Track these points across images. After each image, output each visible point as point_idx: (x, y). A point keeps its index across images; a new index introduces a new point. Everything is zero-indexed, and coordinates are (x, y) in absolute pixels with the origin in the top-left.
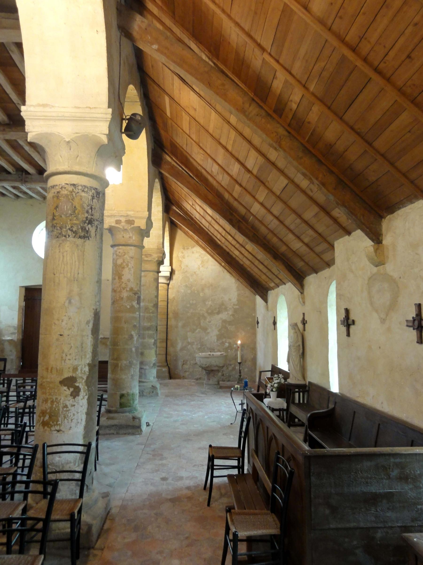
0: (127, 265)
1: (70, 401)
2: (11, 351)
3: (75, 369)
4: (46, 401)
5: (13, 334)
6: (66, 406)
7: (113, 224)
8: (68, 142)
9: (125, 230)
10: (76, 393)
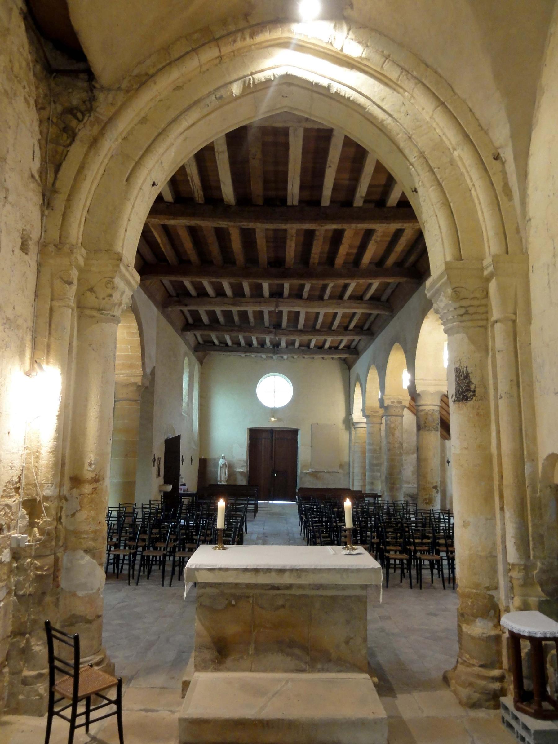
0: (397, 428)
1: (436, 495)
2: (242, 480)
3: (437, 483)
4: (427, 494)
5: (243, 466)
6: (435, 497)
7: (390, 404)
8: (432, 394)
9: (396, 407)
10: (437, 492)
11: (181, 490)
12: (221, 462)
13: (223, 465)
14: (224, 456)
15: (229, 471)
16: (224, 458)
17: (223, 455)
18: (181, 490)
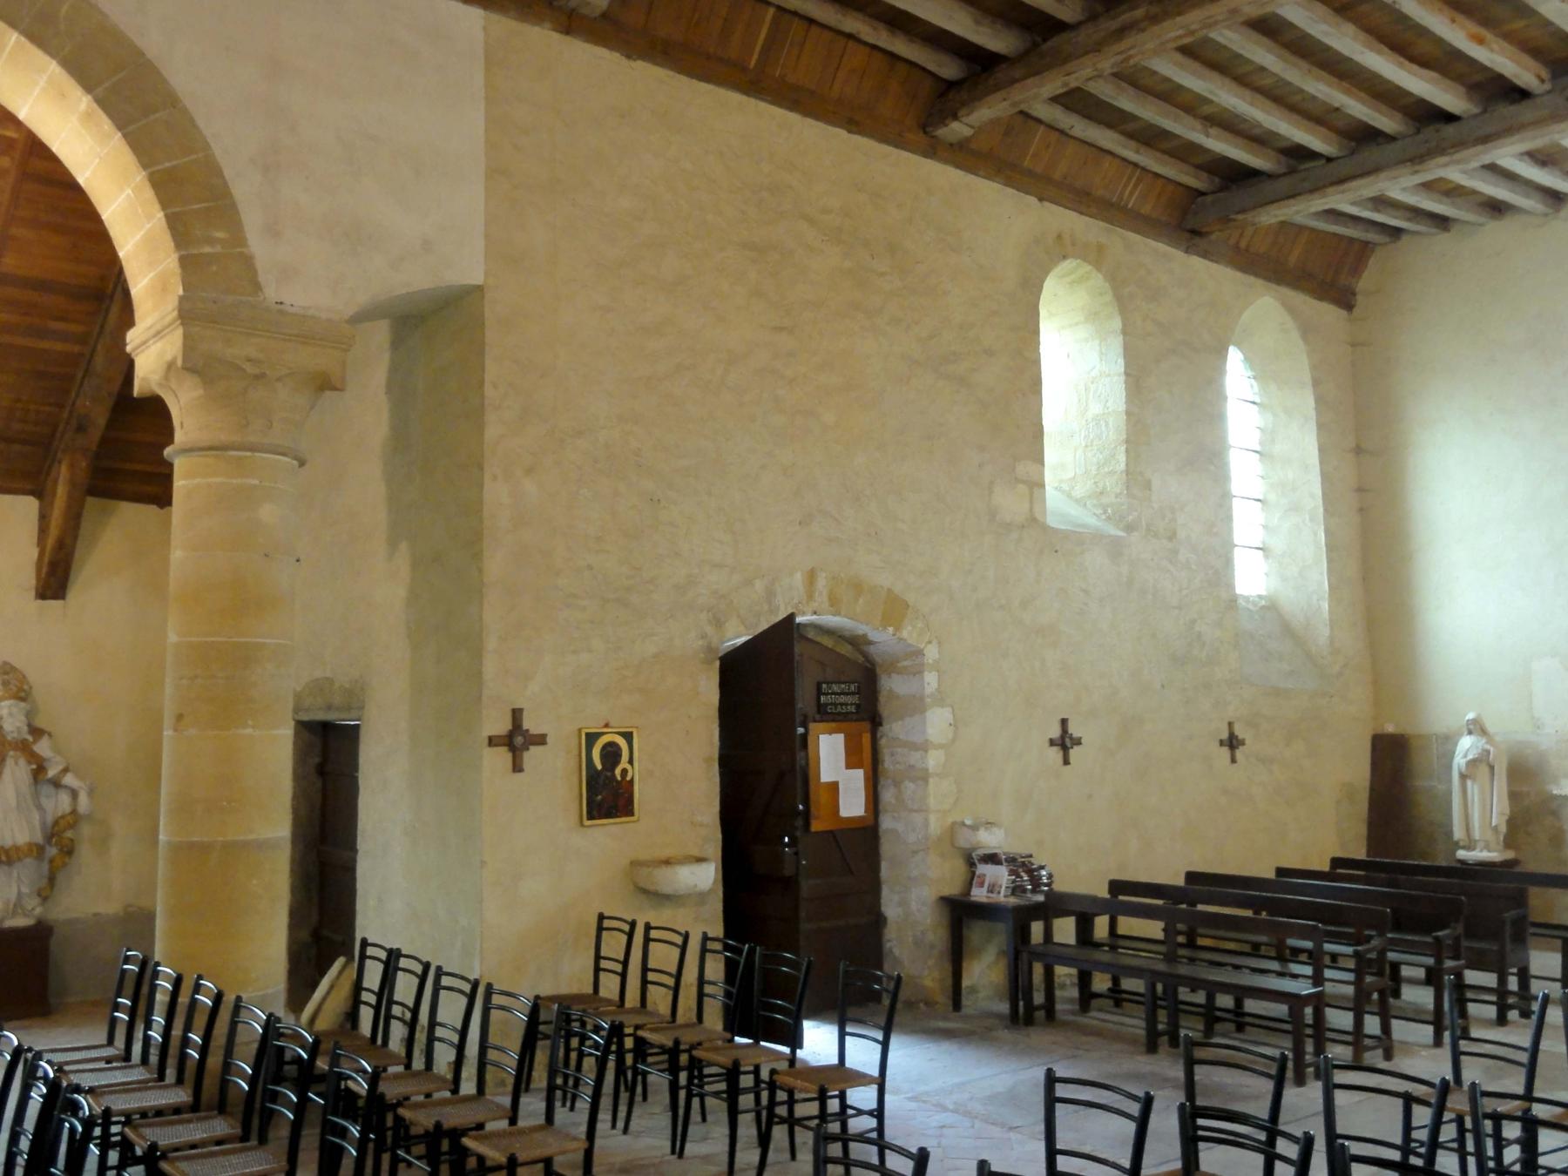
11: (981, 885)
12: (1467, 746)
13: (1473, 763)
14: (1475, 721)
15: (1514, 796)
16: (1477, 728)
17: (1471, 716)
18: (981, 885)
